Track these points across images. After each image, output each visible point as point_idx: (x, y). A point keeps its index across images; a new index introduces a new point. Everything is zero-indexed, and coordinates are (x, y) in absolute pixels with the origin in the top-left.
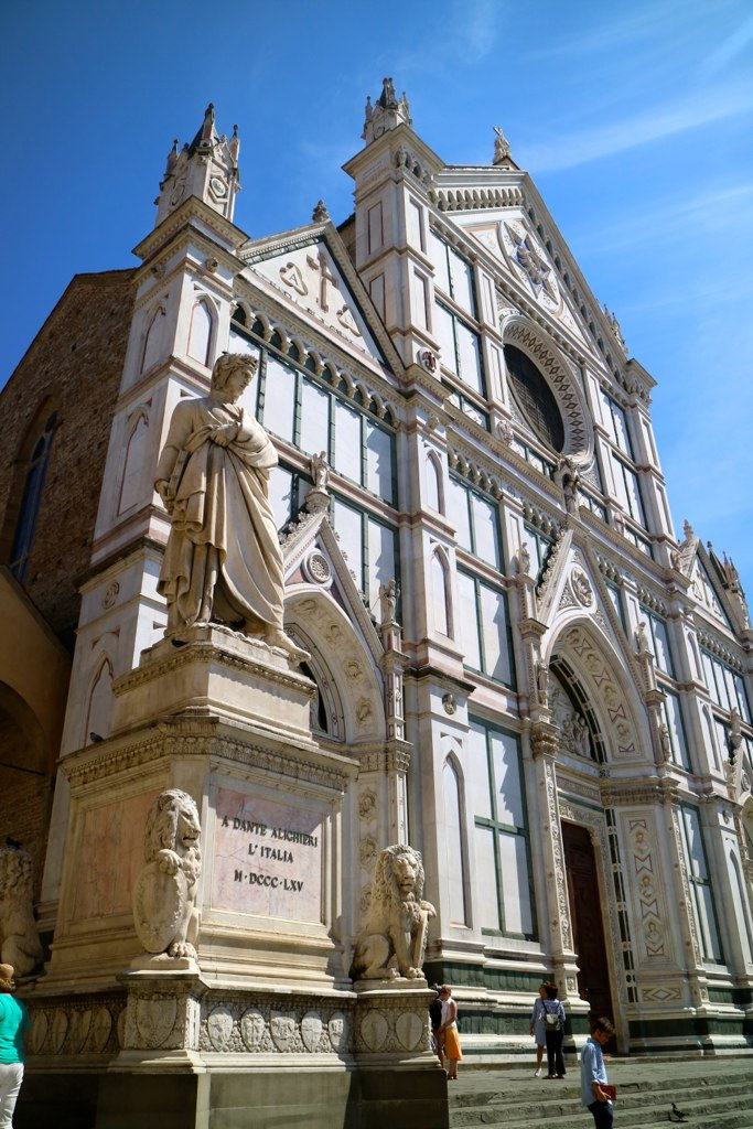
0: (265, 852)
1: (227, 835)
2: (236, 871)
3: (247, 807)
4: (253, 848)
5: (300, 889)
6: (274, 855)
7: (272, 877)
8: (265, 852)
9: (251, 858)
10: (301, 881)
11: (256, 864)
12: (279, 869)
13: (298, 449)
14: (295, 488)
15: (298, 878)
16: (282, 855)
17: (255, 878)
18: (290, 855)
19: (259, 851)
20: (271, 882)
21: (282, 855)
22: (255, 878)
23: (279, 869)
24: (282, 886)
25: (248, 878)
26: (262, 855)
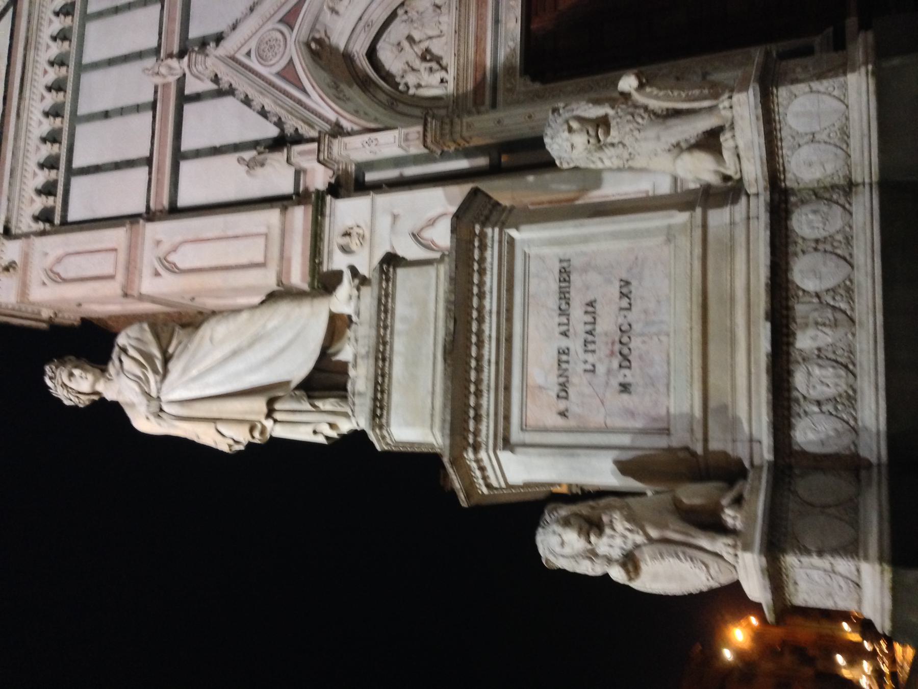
0: (591, 347)
2: (622, 392)
4: (589, 367)
5: (627, 283)
6: (590, 333)
8: (591, 347)
9: (601, 369)
10: (617, 284)
12: (607, 324)
13: (153, 106)
14: (197, 97)
15: (614, 290)
16: (589, 318)
18: (587, 305)
19: (590, 358)
21: (589, 318)
23: (607, 324)
25: (626, 372)
26: (593, 351)
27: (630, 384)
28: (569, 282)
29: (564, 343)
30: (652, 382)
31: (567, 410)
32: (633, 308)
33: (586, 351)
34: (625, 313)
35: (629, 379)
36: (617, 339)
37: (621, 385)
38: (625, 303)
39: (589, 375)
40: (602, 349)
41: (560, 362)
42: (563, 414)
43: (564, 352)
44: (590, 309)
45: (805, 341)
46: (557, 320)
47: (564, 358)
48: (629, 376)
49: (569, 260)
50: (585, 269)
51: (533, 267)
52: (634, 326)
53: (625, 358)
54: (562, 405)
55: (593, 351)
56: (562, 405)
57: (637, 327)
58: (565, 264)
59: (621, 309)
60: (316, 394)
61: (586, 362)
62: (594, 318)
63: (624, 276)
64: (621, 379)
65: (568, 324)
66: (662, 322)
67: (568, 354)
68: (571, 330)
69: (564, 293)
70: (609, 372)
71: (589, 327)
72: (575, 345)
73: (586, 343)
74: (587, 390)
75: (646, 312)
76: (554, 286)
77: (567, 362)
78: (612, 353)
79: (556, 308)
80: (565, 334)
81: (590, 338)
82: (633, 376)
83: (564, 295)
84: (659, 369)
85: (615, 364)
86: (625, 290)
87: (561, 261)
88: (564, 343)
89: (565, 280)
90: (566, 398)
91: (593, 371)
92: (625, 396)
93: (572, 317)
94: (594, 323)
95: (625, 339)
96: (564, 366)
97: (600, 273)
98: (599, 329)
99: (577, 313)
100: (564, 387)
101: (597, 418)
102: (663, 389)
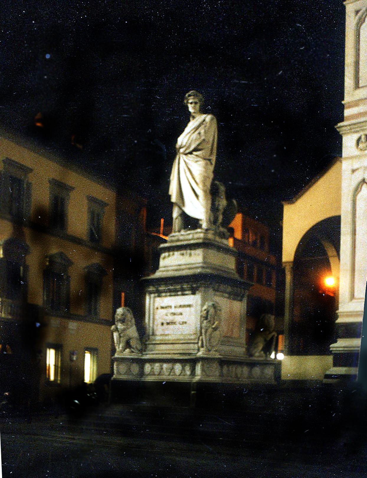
11: (170, 318)
12: (178, 319)
15: (185, 320)
17: (168, 324)
22: (168, 324)
23: (178, 319)
45: (165, 366)
48: (165, 325)
54: (159, 308)
56: (159, 308)
72: (173, 310)
76: (187, 303)
80: (175, 307)
83: (184, 306)
84: (167, 332)
85: (168, 321)
88: (173, 308)
92: (160, 324)
98: (175, 316)
101: (157, 317)
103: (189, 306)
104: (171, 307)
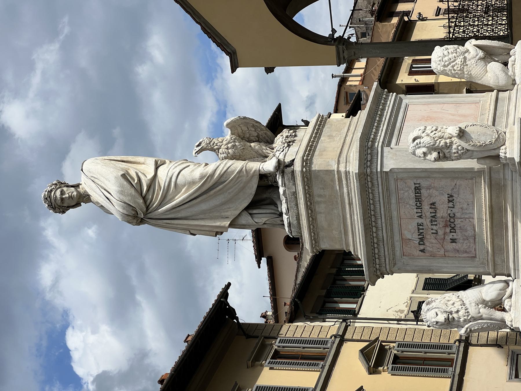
1: (431, 249)
2: (451, 242)
3: (409, 237)
4: (434, 231)
5: (452, 196)
7: (449, 217)
8: (434, 223)
9: (441, 232)
10: (447, 196)
12: (443, 212)
15: (445, 198)
16: (432, 210)
17: (453, 229)
18: (431, 204)
19: (434, 227)
20: (453, 217)
24: (454, 210)
26: (436, 225)
27: (456, 239)
28: (420, 194)
29: (420, 221)
30: (467, 238)
31: (424, 249)
32: (455, 207)
33: (432, 225)
34: (452, 209)
35: (455, 237)
36: (448, 219)
37: (451, 239)
38: (451, 204)
39: (434, 235)
40: (442, 224)
41: (419, 229)
42: (422, 251)
43: (420, 225)
44: (433, 207)
46: (415, 210)
47: (421, 227)
49: (420, 184)
50: (428, 188)
51: (400, 184)
52: (456, 215)
53: (453, 228)
54: (422, 247)
55: (436, 225)
56: (422, 247)
57: (458, 215)
58: (417, 185)
59: (449, 207)
60: (255, 211)
61: (432, 229)
62: (436, 211)
63: (450, 192)
64: (451, 237)
65: (422, 213)
66: (470, 213)
67: (423, 226)
68: (424, 215)
69: (418, 199)
70: (445, 234)
71: (433, 214)
72: (426, 222)
73: (431, 221)
74: (434, 241)
75: (462, 208)
76: (413, 195)
77: (423, 229)
78: (446, 226)
79: (414, 204)
80: (420, 217)
81: (434, 219)
82: (457, 236)
83: (418, 199)
85: (448, 230)
86: (451, 199)
87: (415, 184)
88: (420, 221)
89: (418, 193)
90: (424, 244)
91: (437, 233)
92: (454, 244)
93: (423, 210)
94: (435, 213)
95: (452, 220)
96: (421, 231)
97: (437, 190)
99: (426, 207)
100: (422, 240)
102: (472, 241)
103: (418, 189)
104: (419, 225)
